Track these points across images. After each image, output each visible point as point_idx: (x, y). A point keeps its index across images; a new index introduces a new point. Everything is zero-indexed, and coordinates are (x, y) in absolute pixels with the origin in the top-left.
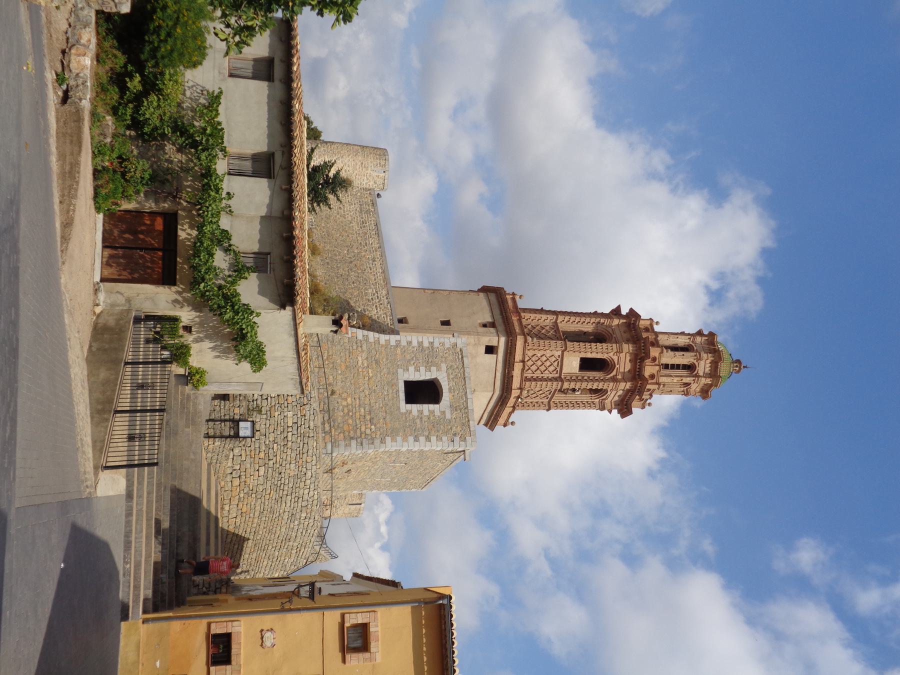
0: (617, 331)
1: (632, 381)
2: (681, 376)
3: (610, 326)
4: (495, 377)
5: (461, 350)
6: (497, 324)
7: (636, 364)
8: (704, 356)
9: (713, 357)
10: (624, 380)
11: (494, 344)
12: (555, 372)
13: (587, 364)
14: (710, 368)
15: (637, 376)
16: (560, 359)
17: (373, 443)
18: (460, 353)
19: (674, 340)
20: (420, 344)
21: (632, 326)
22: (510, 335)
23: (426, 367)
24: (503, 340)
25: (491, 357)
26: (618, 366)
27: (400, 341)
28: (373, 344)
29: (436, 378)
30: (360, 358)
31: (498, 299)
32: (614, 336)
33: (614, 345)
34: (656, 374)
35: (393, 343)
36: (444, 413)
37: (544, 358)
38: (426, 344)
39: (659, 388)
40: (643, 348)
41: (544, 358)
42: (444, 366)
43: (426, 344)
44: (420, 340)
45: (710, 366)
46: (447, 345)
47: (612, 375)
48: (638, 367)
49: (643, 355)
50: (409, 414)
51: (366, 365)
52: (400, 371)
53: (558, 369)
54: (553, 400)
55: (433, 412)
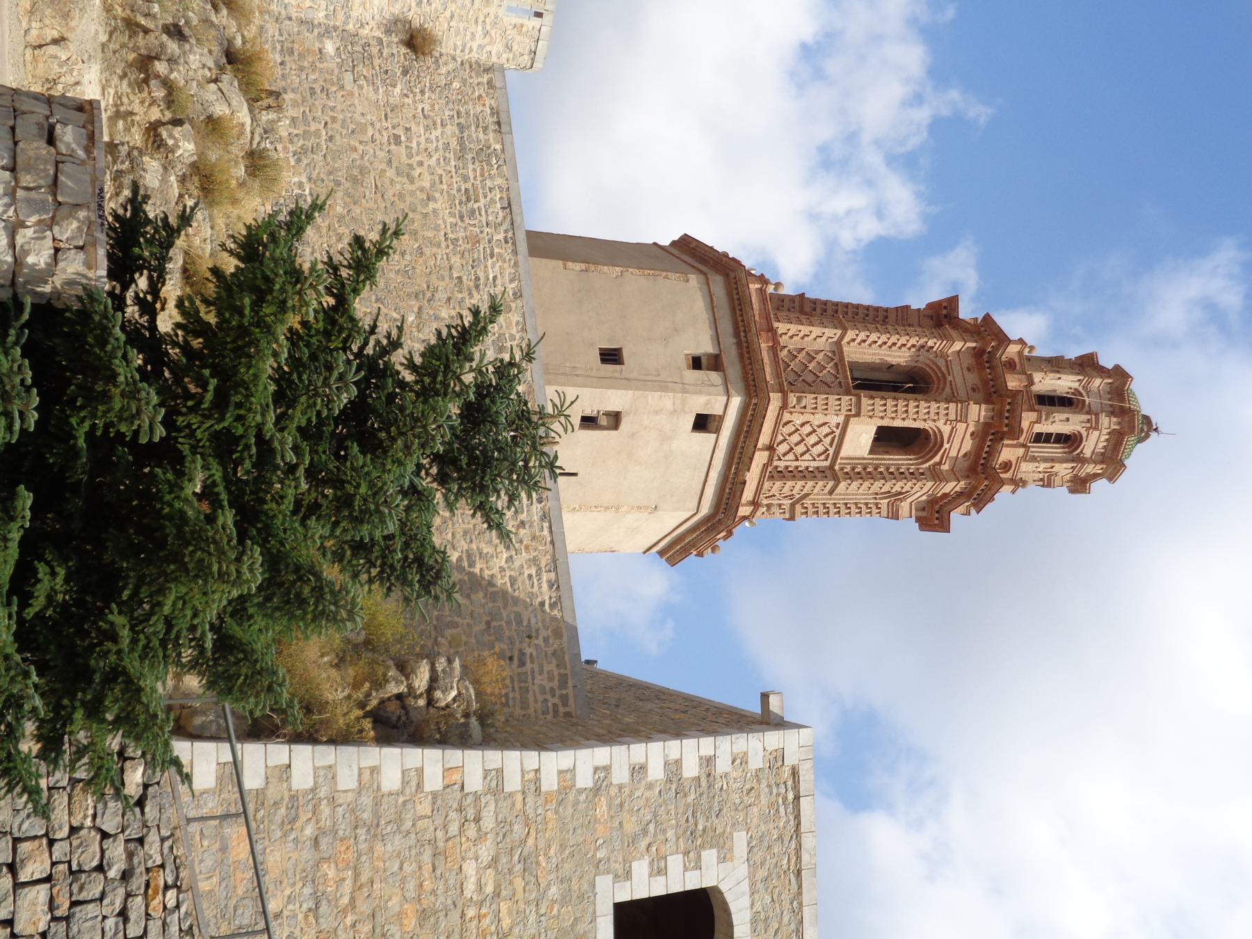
0: (956, 368)
1: (968, 477)
2: (1052, 460)
3: (943, 356)
4: (706, 481)
5: (795, 773)
7: (984, 441)
8: (1105, 421)
9: (1119, 423)
10: (954, 474)
11: (717, 410)
12: (823, 457)
13: (887, 438)
14: (1105, 444)
15: (980, 467)
16: (838, 432)
18: (790, 783)
19: (1053, 381)
20: (673, 768)
21: (985, 357)
22: (754, 389)
23: (686, 853)
24: (736, 402)
25: (705, 440)
26: (946, 446)
27: (607, 769)
31: (730, 295)
32: (950, 378)
33: (952, 406)
35: (585, 780)
37: (807, 429)
38: (691, 769)
40: (1007, 414)
41: (807, 429)
42: (740, 841)
44: (674, 755)
45: (1107, 440)
48: (986, 449)
49: (1005, 429)
51: (489, 889)
52: (604, 883)
53: (831, 451)
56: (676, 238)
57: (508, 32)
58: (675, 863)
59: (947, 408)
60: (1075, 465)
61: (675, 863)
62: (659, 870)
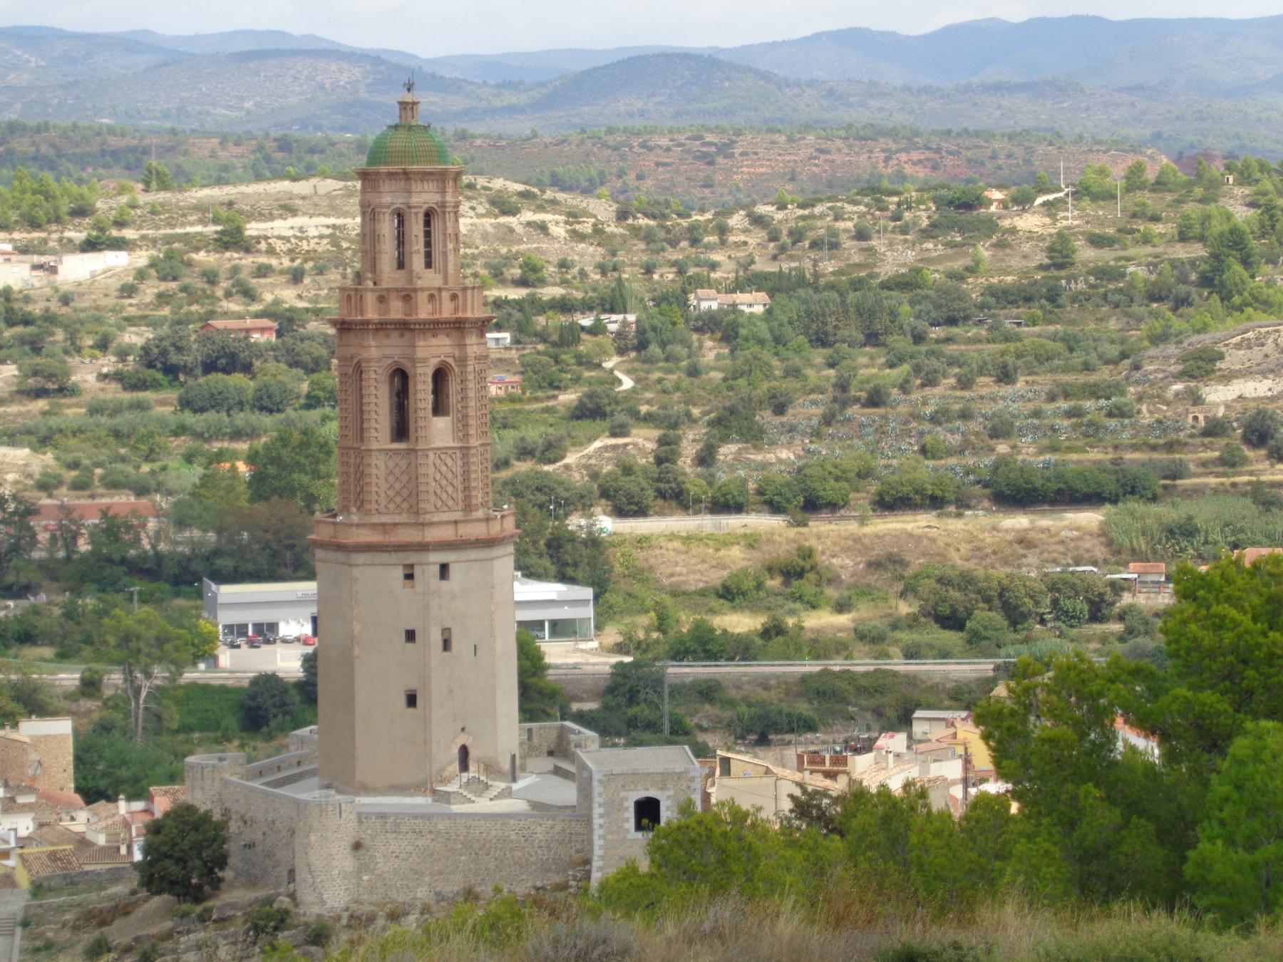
0: (388, 351)
6: (408, 562)
11: (437, 569)
20: (601, 816)
25: (454, 571)
35: (602, 842)
36: (668, 797)
38: (601, 810)
42: (623, 794)
43: (601, 810)
46: (601, 789)
47: (453, 364)
52: (629, 836)
58: (626, 815)
61: (626, 815)
62: (627, 820)
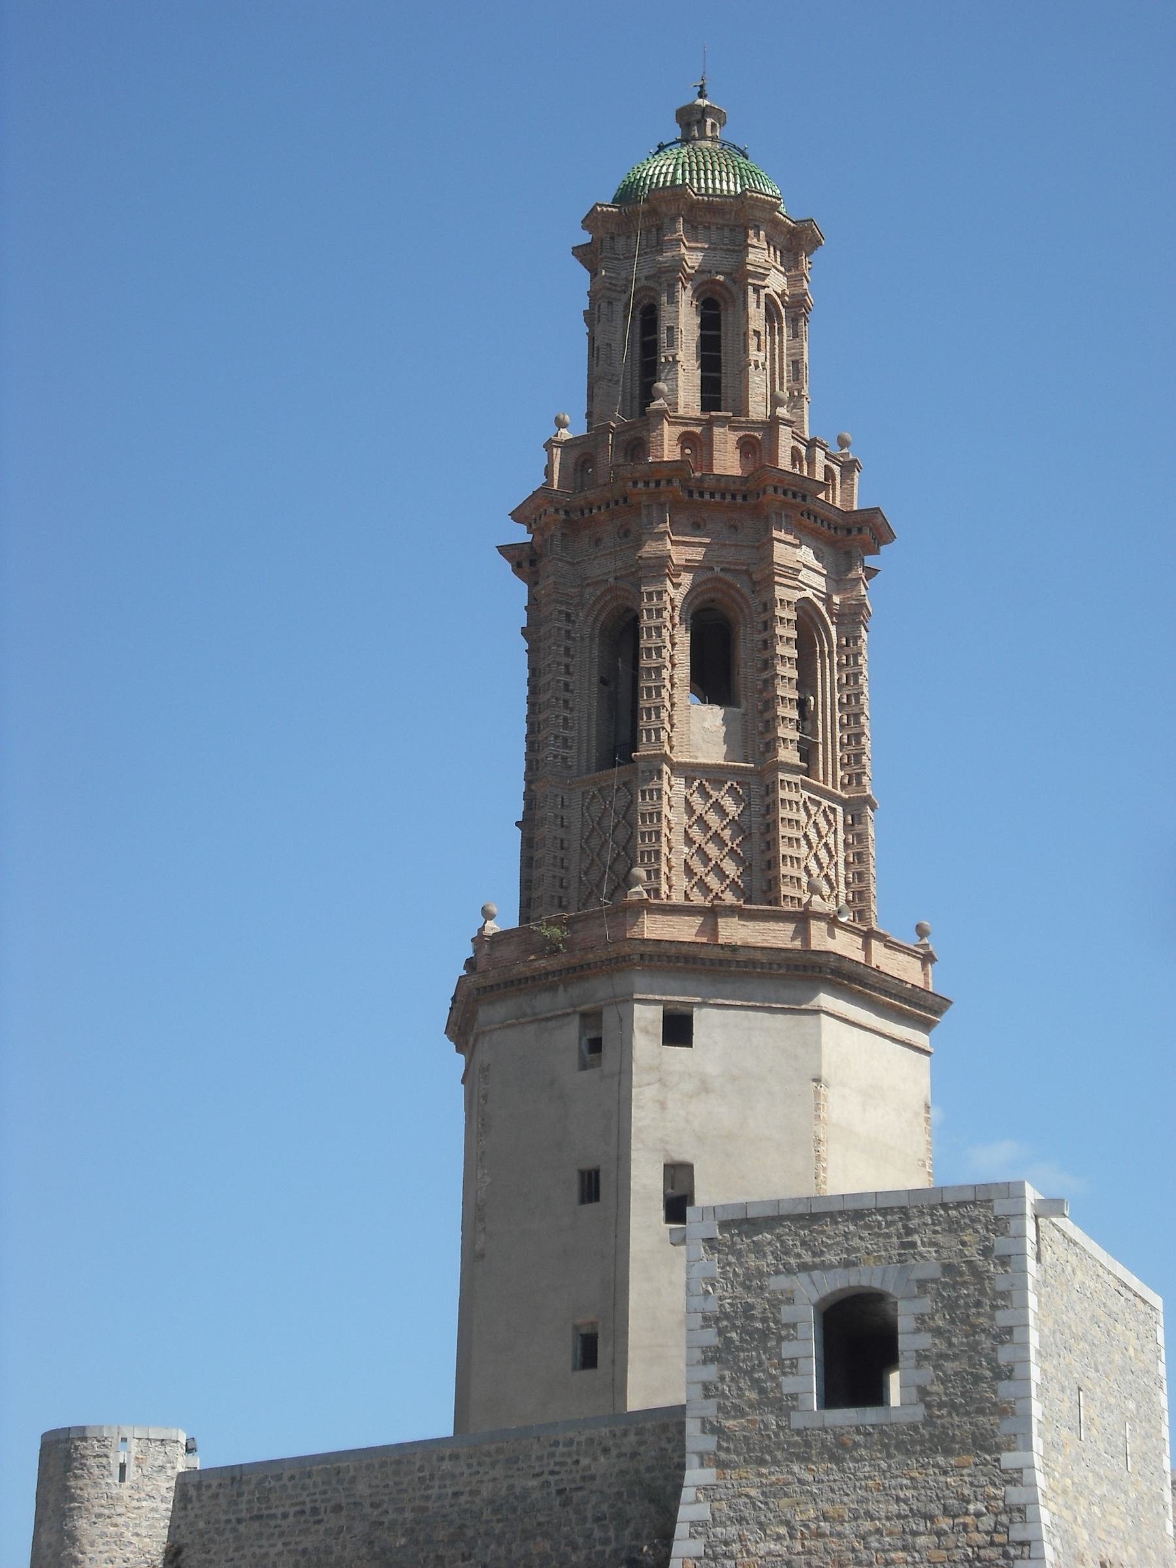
9: (674, 220)
17: (1021, 1510)
23: (780, 1339)
25: (705, 1021)
27: (704, 1421)
28: (716, 1504)
29: (816, 1306)
30: (762, 1548)
34: (742, 433)
37: (696, 833)
39: (789, 423)
41: (696, 833)
42: (778, 1283)
49: (676, 483)
50: (929, 1394)
51: (783, 1530)
52: (797, 1421)
54: (839, 792)
55: (920, 1318)
56: (452, 1046)
57: (146, 1473)
59: (650, 594)
60: (750, 289)
